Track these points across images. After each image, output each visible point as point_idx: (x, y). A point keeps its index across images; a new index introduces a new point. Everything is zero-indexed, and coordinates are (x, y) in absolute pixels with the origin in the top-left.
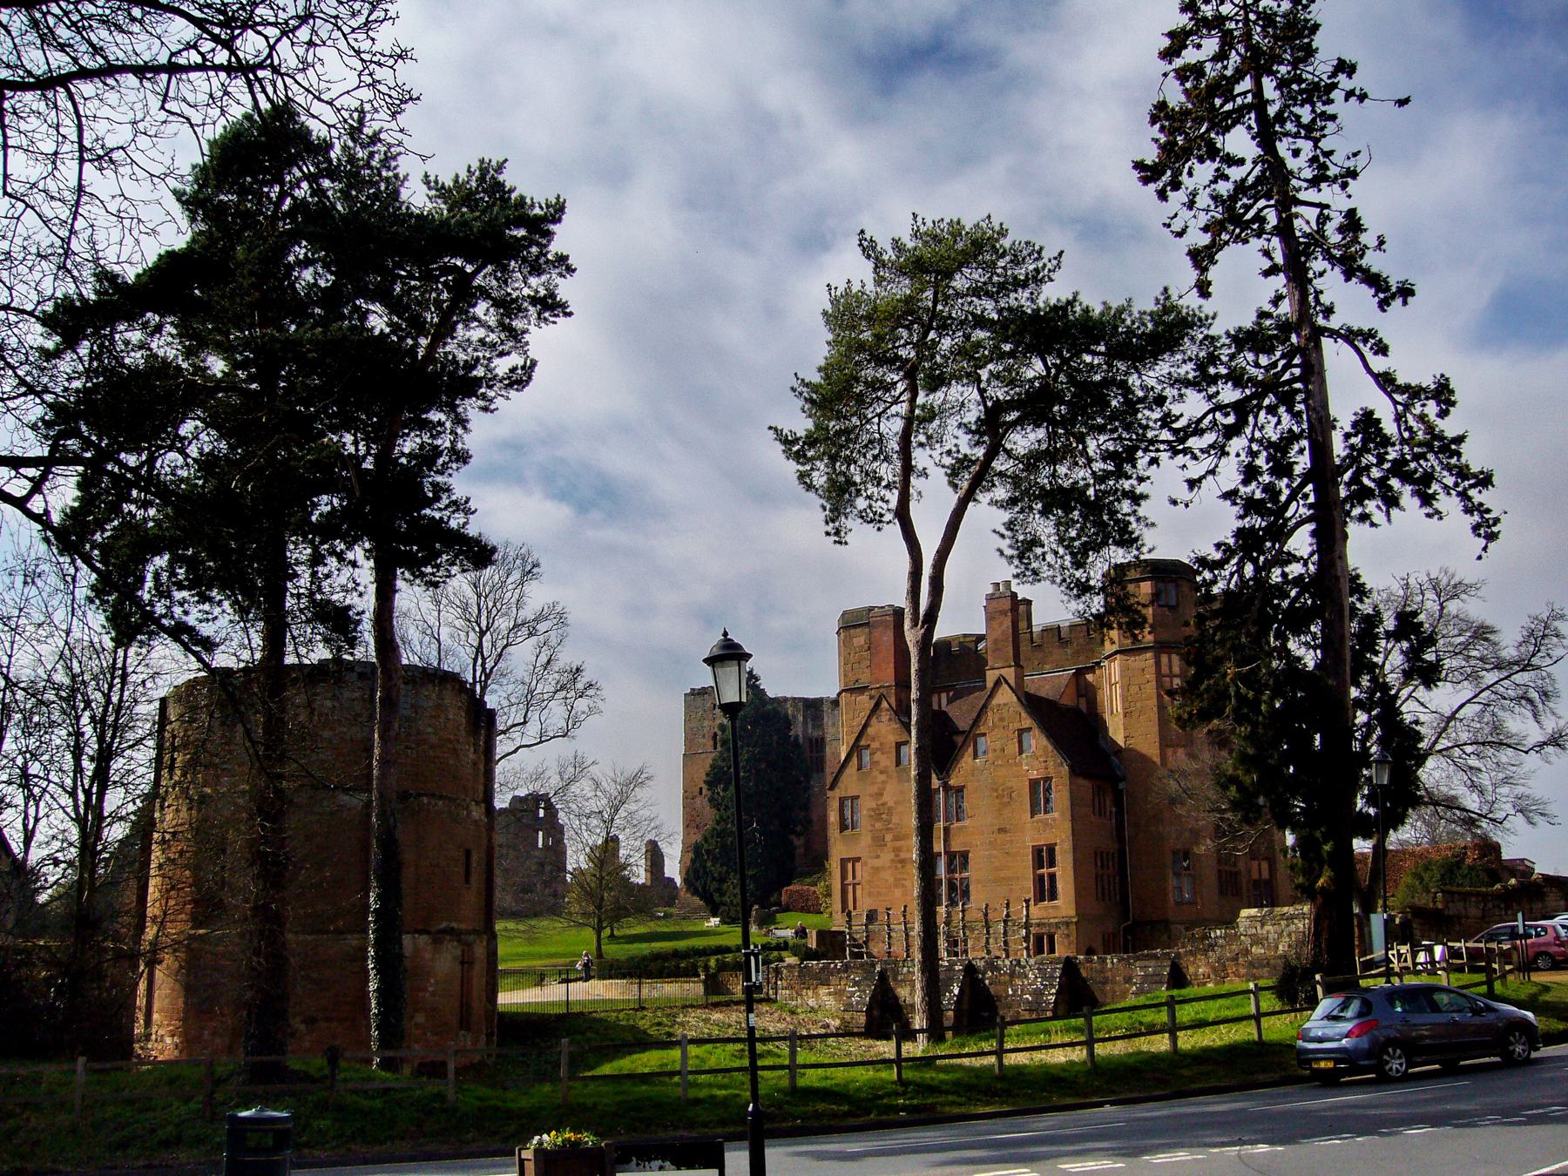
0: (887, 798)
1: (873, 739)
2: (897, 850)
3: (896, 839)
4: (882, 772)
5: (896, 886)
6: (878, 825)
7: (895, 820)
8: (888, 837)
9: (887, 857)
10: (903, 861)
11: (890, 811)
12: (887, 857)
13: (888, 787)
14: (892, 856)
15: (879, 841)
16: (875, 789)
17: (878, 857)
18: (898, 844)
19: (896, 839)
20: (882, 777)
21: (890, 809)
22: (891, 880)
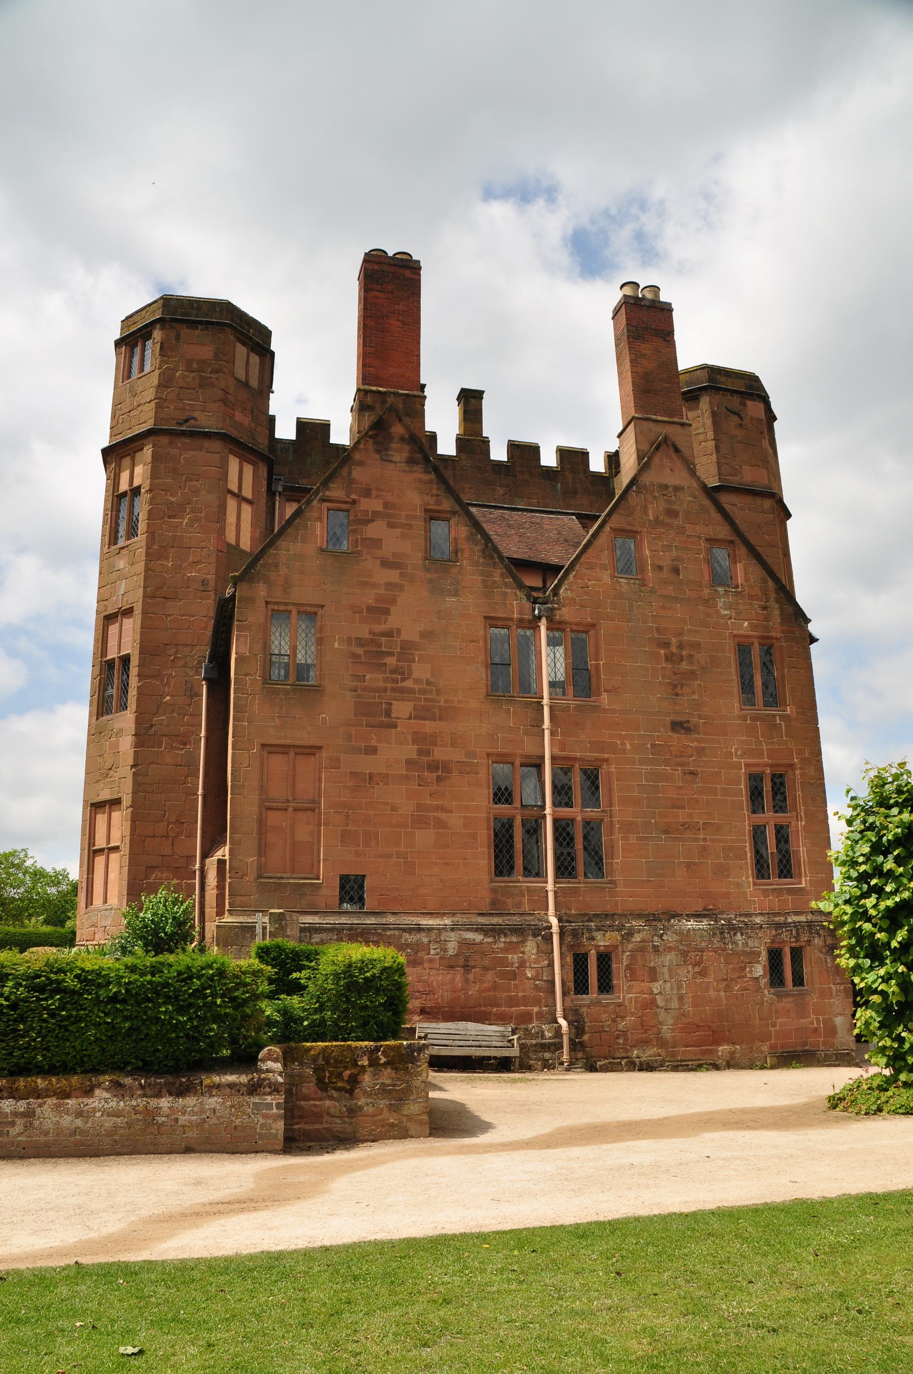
0: (406, 619)
1: (367, 493)
2: (425, 742)
3: (422, 713)
4: (385, 564)
5: (420, 820)
6: (375, 679)
7: (421, 671)
8: (402, 709)
9: (395, 752)
10: (441, 769)
11: (407, 651)
12: (395, 752)
14: (410, 751)
15: (374, 715)
17: (373, 751)
18: (429, 727)
19: (422, 713)
20: (393, 575)
21: (407, 648)
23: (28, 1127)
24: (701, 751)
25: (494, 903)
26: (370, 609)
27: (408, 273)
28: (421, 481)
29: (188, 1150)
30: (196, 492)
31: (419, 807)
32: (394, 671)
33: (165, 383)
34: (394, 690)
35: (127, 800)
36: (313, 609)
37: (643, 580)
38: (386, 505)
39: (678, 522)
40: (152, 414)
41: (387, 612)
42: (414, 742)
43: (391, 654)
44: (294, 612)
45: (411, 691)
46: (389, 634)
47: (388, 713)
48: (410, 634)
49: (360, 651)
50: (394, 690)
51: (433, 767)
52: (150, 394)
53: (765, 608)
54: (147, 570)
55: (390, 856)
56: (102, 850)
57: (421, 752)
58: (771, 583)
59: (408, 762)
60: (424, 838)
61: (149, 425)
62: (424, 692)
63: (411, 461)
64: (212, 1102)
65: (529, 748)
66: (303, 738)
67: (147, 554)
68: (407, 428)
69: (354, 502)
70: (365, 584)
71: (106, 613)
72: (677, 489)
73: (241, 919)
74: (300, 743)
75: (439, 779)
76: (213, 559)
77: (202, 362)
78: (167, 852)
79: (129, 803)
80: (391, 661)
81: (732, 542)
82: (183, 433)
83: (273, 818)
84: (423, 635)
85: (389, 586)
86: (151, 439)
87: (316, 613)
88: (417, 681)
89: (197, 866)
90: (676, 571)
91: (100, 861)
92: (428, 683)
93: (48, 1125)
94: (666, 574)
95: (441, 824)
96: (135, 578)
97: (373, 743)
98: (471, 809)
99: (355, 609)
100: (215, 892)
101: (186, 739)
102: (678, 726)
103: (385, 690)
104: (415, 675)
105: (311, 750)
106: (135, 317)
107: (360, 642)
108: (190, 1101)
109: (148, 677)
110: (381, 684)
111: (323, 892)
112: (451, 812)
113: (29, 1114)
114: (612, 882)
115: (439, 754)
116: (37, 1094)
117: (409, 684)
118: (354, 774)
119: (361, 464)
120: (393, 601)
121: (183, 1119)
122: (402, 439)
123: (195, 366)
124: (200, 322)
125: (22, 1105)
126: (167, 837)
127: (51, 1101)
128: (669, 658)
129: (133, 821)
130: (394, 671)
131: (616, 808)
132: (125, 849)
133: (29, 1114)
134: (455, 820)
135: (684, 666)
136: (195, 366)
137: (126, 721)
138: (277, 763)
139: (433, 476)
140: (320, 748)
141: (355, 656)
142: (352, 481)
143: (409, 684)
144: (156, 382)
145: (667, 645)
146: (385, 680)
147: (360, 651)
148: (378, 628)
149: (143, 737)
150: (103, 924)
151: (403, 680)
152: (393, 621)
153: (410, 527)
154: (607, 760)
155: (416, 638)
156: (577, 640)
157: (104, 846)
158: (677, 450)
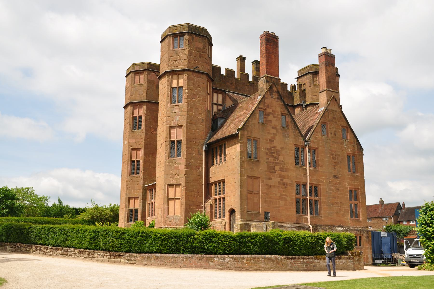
0: (277, 144)
3: (281, 170)
4: (273, 128)
5: (281, 198)
6: (271, 159)
7: (281, 158)
8: (277, 168)
9: (276, 180)
12: (276, 180)
13: (277, 138)
14: (279, 180)
15: (271, 169)
16: (269, 137)
17: (271, 179)
18: (283, 173)
19: (281, 170)
20: (274, 131)
21: (278, 151)
22: (279, 195)
23: (319, 265)
24: (340, 184)
25: (297, 221)
26: (270, 140)
27: (275, 40)
28: (280, 104)
29: (341, 270)
30: (199, 91)
31: (281, 195)
32: (275, 158)
33: (190, 54)
34: (275, 163)
35: (183, 184)
36: (256, 139)
37: (328, 136)
38: (273, 111)
39: (336, 121)
40: (187, 63)
41: (273, 141)
42: (280, 177)
43: (274, 153)
44: (253, 140)
45: (279, 163)
46: (274, 147)
47: (274, 169)
48: (278, 148)
49: (268, 152)
50: (275, 163)
51: (284, 184)
52: (185, 57)
53: (354, 146)
54: (187, 115)
55: (275, 207)
56: (172, 199)
57: (282, 180)
58: (355, 139)
59: (279, 182)
60: (282, 203)
61: (185, 67)
62: (282, 164)
63: (278, 98)
64: (344, 261)
65: (304, 181)
66: (256, 175)
67: (187, 110)
68: (277, 89)
69: (265, 109)
70: (268, 133)
71: (171, 125)
72: (336, 111)
73: (244, 222)
74: (256, 176)
75: (285, 187)
76: (204, 113)
77: (200, 48)
78: (195, 201)
79: (185, 185)
80: (274, 155)
81: (347, 127)
82: (196, 72)
83: (249, 195)
84: (282, 148)
85: (274, 134)
86: (187, 72)
87: (257, 140)
88: (280, 161)
89: (203, 205)
90: (335, 134)
91: (171, 203)
92: (283, 161)
93: (322, 264)
94: (333, 135)
95: (286, 199)
96: (183, 116)
97: (271, 177)
98: (292, 195)
99: (266, 140)
100: (209, 213)
101: (199, 168)
102: (335, 176)
103: (273, 163)
104: (280, 159)
105: (257, 178)
106: (176, 28)
107: (268, 149)
108: (341, 260)
109: (189, 148)
110: (272, 161)
111: (261, 216)
112: (287, 196)
113: (319, 262)
114: (321, 217)
115: (286, 181)
116: (320, 259)
117: (278, 161)
118: (267, 185)
119: (267, 98)
120: (275, 138)
121: (340, 264)
122: (276, 92)
123: (198, 49)
124: (199, 35)
125: (318, 261)
126: (195, 196)
127: (322, 260)
128: (333, 158)
129: (186, 191)
130: (275, 158)
131: (322, 197)
132: (183, 199)
133: (319, 262)
134: (288, 198)
135: (336, 161)
136: (198, 49)
137: (182, 160)
138: (250, 180)
139: (282, 103)
140: (259, 177)
141: (267, 153)
142: (265, 103)
143: (278, 161)
144: (187, 53)
145: (333, 155)
146: (274, 160)
147: (268, 152)
148: (272, 146)
149: (188, 166)
150: (175, 221)
151: (277, 160)
152: (275, 144)
153: (278, 117)
154: (320, 185)
155: (280, 149)
156: (313, 151)
157: (173, 197)
158: (336, 100)
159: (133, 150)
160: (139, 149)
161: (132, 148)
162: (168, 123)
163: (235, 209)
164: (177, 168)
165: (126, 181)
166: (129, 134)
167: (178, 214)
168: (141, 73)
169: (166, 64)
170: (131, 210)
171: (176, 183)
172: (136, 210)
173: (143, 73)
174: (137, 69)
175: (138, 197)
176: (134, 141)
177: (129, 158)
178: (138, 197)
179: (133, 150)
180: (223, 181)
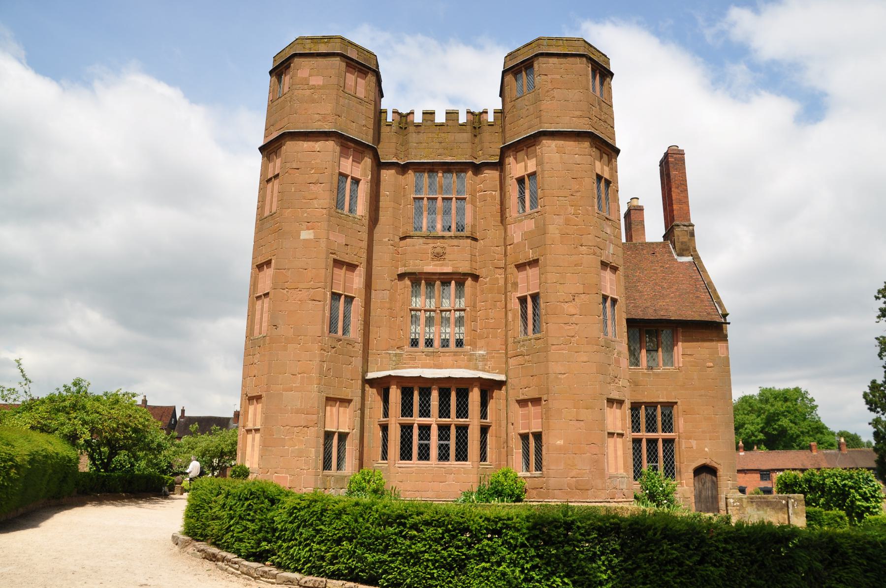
159: (338, 263)
160: (352, 267)
161: (335, 256)
162: (598, 251)
163: (716, 466)
164: (617, 361)
165: (316, 346)
166: (330, 215)
167: (621, 471)
168: (360, 71)
169: (578, 113)
170: (329, 435)
171: (617, 397)
172: (343, 437)
173: (366, 74)
174: (353, 54)
175: (349, 401)
176: (341, 239)
177: (329, 284)
178: (349, 401)
179: (338, 263)
180: (669, 406)
